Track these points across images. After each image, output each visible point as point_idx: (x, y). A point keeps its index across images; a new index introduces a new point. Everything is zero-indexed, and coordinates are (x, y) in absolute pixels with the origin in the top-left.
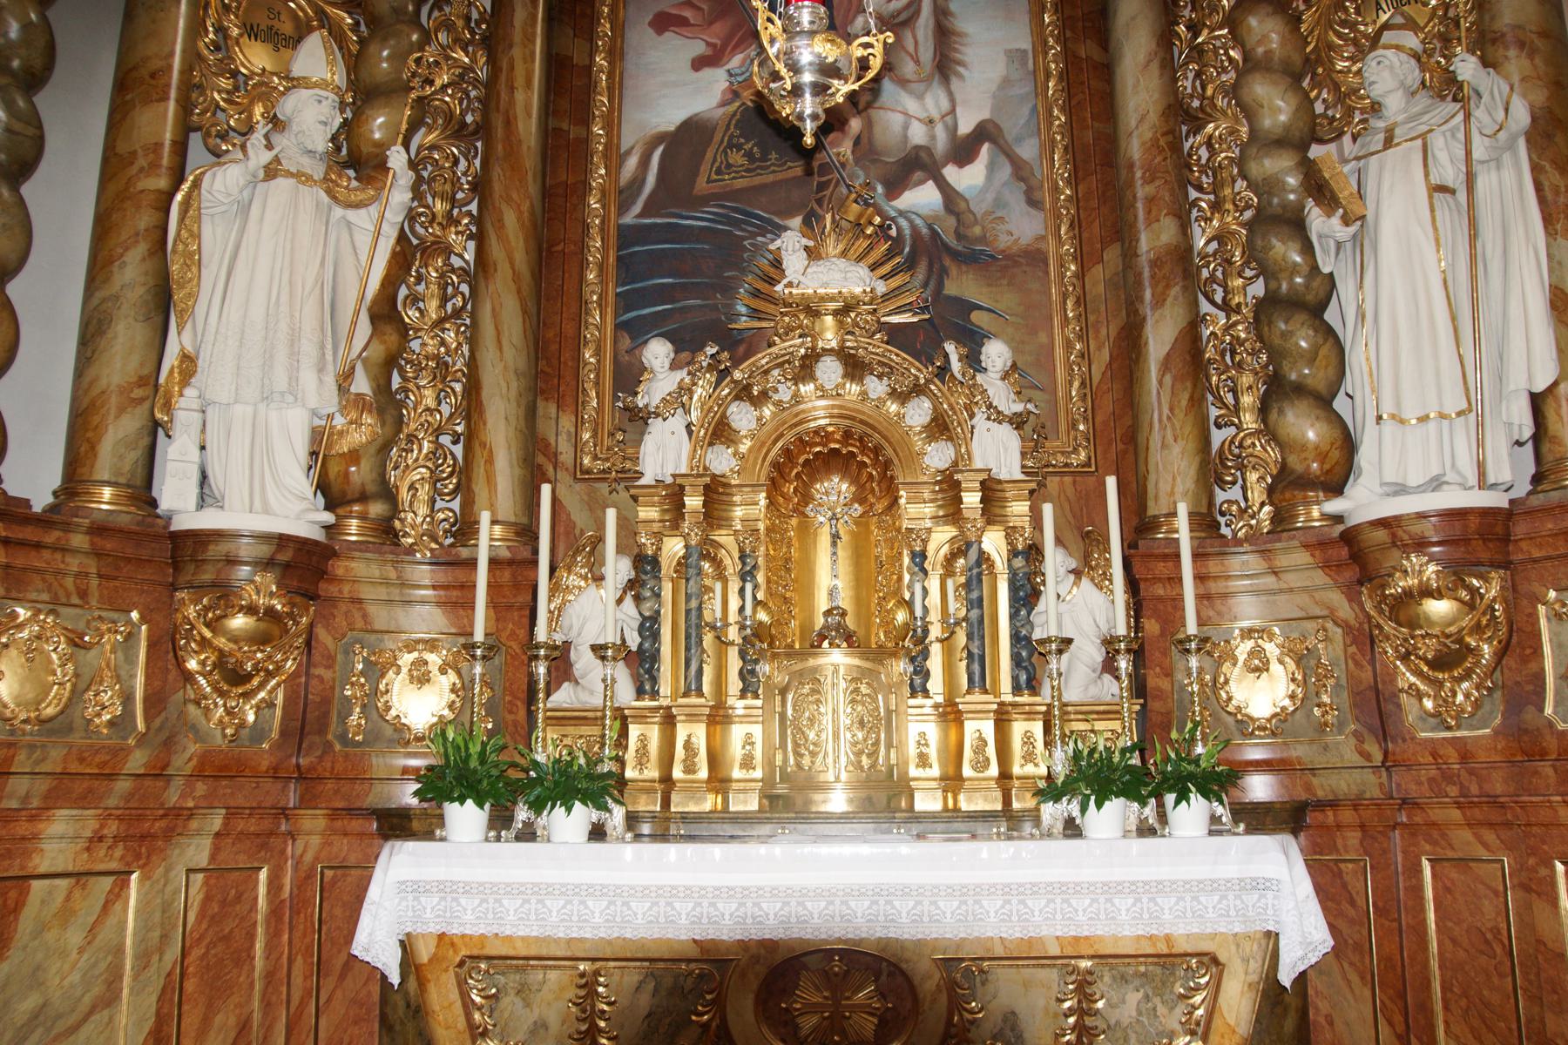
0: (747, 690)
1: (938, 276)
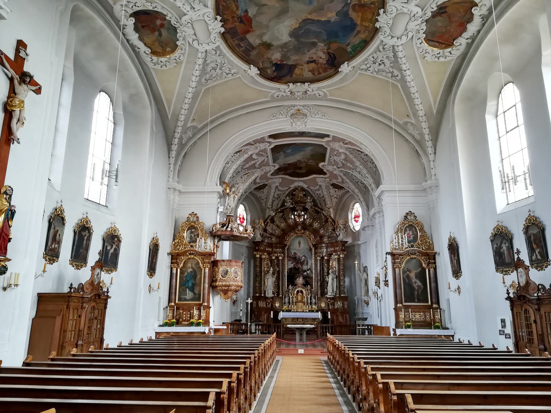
0: (295, 305)
1: (306, 279)
